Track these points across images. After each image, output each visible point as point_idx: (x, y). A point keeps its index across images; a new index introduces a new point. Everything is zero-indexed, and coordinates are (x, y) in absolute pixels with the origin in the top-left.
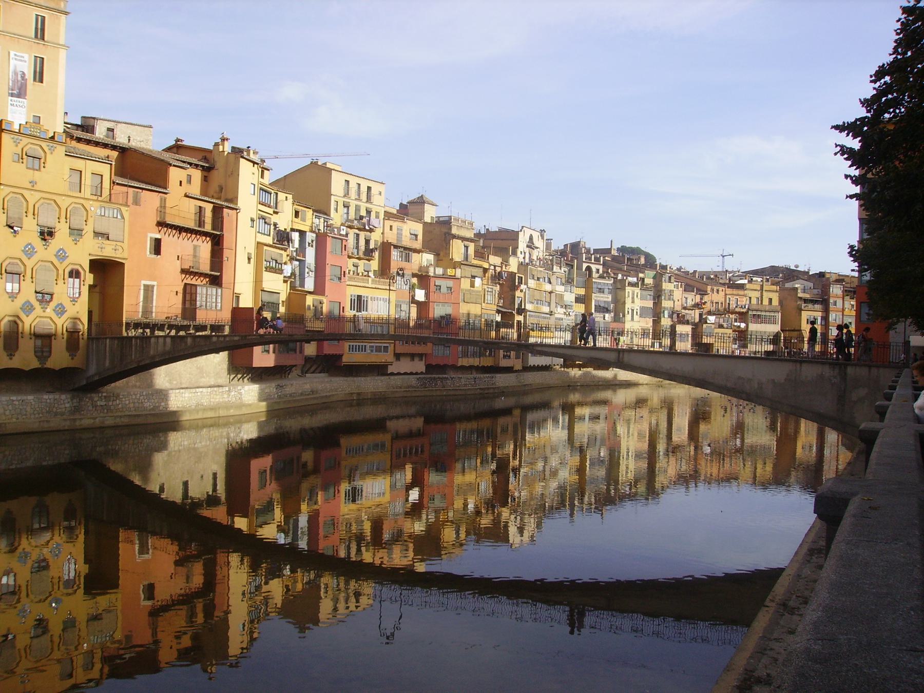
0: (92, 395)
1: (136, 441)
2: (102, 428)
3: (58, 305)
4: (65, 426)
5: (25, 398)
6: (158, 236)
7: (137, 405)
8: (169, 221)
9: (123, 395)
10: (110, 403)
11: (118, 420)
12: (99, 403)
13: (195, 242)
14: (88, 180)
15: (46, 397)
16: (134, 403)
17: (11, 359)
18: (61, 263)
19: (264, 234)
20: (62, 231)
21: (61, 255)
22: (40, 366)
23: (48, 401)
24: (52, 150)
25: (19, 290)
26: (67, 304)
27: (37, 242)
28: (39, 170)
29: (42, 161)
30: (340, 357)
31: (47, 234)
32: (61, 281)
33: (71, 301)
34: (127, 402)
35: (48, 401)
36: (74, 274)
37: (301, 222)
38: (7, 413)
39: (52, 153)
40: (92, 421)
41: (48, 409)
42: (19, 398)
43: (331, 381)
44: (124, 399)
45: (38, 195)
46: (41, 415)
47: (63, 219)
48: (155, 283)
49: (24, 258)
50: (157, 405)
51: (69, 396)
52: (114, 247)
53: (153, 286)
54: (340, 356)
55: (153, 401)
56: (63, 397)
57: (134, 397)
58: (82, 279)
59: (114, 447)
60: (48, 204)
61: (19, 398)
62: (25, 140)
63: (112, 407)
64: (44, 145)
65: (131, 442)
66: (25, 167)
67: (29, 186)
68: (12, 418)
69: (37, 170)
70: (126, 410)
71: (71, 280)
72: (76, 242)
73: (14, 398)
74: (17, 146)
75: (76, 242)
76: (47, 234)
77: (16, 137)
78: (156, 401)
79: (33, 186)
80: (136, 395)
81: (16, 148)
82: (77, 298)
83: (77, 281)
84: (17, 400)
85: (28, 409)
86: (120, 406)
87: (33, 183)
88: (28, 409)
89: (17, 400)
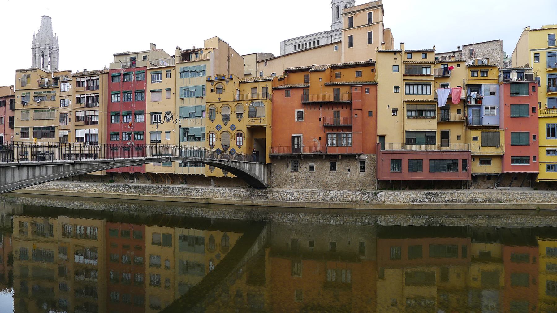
0: (257, 190)
1: (283, 216)
2: (257, 206)
4: (237, 203)
5: (224, 189)
6: (302, 110)
7: (283, 197)
8: (311, 100)
9: (275, 192)
10: (268, 195)
11: (266, 203)
12: (261, 194)
13: (336, 109)
14: (260, 90)
15: (234, 189)
16: (282, 196)
17: (212, 173)
18: (233, 131)
19: (418, 94)
20: (233, 117)
21: (233, 128)
22: (224, 176)
23: (235, 191)
24: (227, 83)
26: (236, 149)
27: (222, 124)
29: (223, 89)
30: (535, 175)
31: (226, 118)
32: (233, 140)
34: (277, 195)
35: (235, 191)
36: (240, 135)
37: (482, 78)
38: (217, 195)
39: (227, 85)
40: (251, 202)
41: (235, 195)
43: (524, 193)
44: (275, 194)
45: (222, 104)
46: (232, 197)
47: (233, 112)
48: (301, 135)
49: (216, 131)
50: (297, 198)
51: (245, 190)
52: (260, 120)
53: (301, 136)
54: (536, 174)
55: (293, 196)
56: (242, 190)
57: (281, 192)
58: (243, 135)
59: (270, 216)
62: (215, 83)
63: (269, 197)
64: (224, 82)
65: (280, 216)
67: (218, 101)
68: (219, 197)
70: (277, 199)
71: (238, 138)
72: (239, 120)
73: (220, 189)
74: (212, 86)
75: (239, 120)
76: (226, 118)
77: (212, 82)
78: (296, 196)
79: (219, 100)
80: (283, 192)
82: (241, 146)
84: (221, 190)
85: (226, 194)
86: (273, 197)
87: (219, 99)
88: (226, 194)
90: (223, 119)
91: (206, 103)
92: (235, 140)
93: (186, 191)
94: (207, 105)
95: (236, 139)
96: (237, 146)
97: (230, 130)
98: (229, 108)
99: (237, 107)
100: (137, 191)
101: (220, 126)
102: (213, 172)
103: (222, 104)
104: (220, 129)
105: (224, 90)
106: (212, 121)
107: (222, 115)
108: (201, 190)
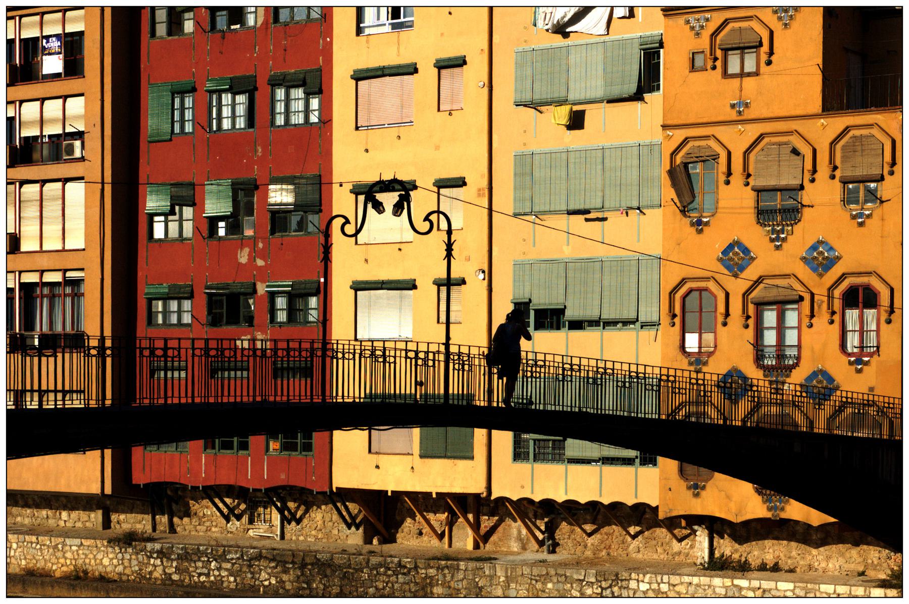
3: (815, 374)
18: (821, 276)
25: (716, 347)
28: (757, 74)
33: (850, 363)
42: (755, 584)
60: (780, 144)
61: (755, 584)
66: (720, 76)
67: (733, 115)
69: (749, 75)
71: (852, 315)
72: (860, 220)
75: (860, 220)
81: (698, 40)
83: (870, 313)
84: (749, 589)
89: (749, 589)
90: (763, 215)
91: (665, 127)
92: (832, 322)
93: (550, 585)
94: (669, 138)
95: (837, 318)
96: (845, 359)
97: (803, 271)
98: (795, 152)
99: (844, 147)
100: (285, 577)
101: (746, 251)
102: (703, 493)
103: (752, 131)
104: (742, 269)
105: (771, 53)
106: (699, 226)
107: (758, 191)
108: (633, 584)
